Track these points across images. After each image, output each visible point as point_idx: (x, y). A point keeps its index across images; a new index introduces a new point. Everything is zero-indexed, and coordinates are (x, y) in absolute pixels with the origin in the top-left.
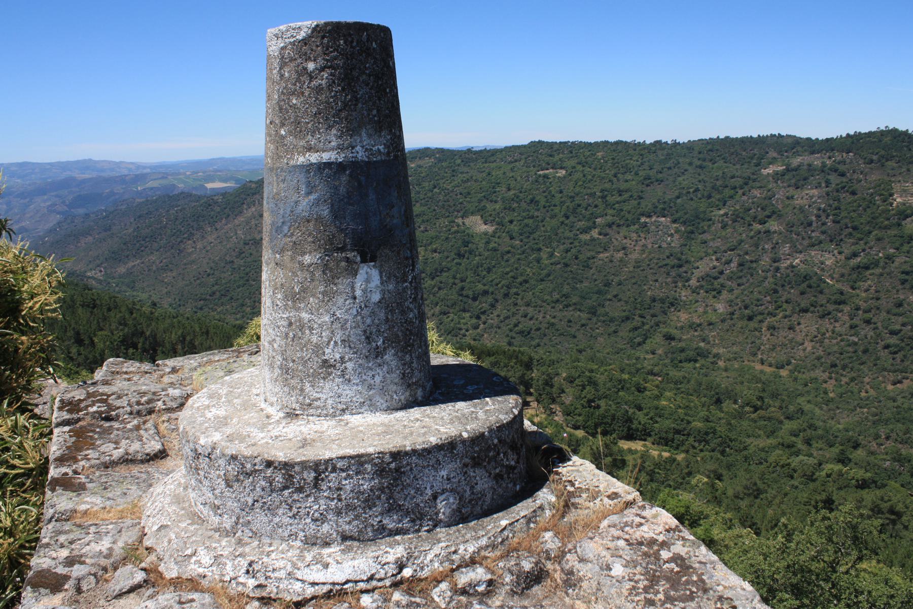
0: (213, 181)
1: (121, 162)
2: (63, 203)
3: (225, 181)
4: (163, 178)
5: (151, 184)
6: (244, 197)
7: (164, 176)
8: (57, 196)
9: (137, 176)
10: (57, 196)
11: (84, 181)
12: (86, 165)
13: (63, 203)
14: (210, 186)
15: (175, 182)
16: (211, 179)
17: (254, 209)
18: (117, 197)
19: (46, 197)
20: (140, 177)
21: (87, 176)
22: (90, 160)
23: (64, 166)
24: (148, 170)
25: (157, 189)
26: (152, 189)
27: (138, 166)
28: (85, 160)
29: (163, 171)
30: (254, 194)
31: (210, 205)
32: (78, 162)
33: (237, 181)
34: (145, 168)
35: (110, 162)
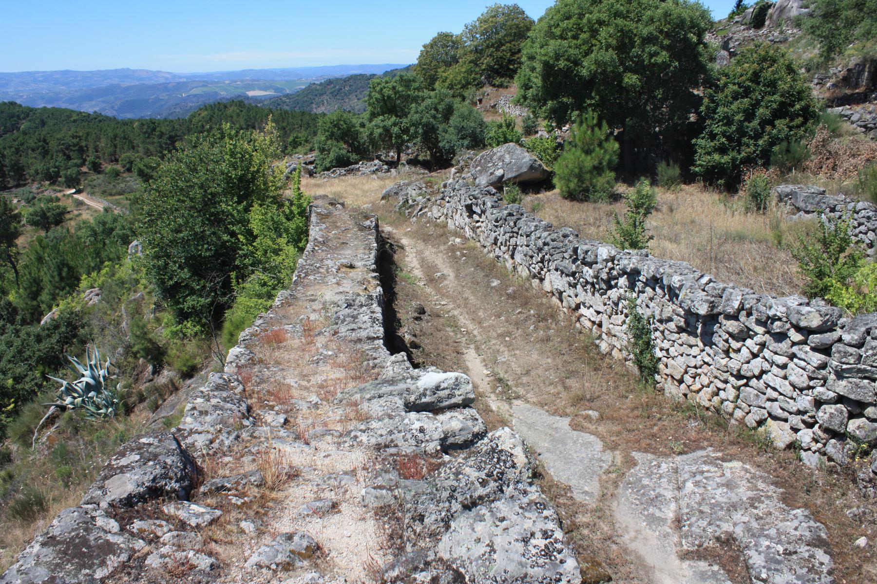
0: (254, 90)
1: (159, 72)
2: (113, 107)
3: (265, 89)
4: (203, 86)
5: (194, 92)
6: (310, 96)
7: (205, 84)
8: (104, 102)
9: (178, 83)
10: (104, 102)
11: (128, 88)
12: (125, 74)
13: (113, 107)
14: (251, 94)
15: (217, 90)
16: (251, 88)
17: (323, 108)
18: (163, 103)
19: (94, 103)
20: (181, 84)
21: (128, 84)
22: (128, 69)
23: (105, 74)
24: (185, 80)
25: (201, 96)
26: (195, 96)
27: (175, 76)
28: (123, 70)
29: (205, 81)
30: (321, 95)
31: (279, 105)
32: (116, 71)
33: (276, 89)
34: (180, 77)
35: (147, 72)
